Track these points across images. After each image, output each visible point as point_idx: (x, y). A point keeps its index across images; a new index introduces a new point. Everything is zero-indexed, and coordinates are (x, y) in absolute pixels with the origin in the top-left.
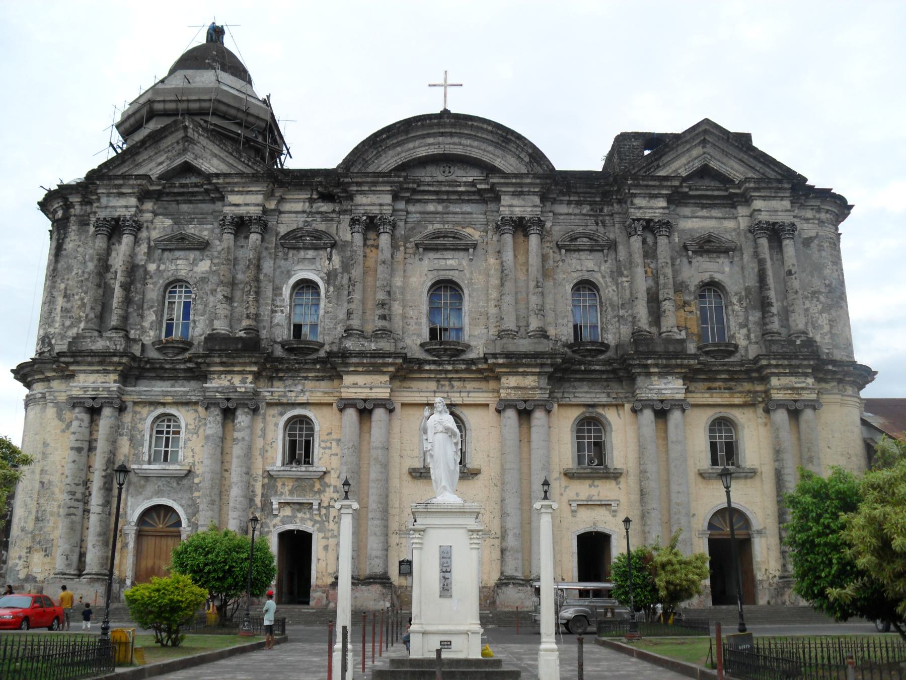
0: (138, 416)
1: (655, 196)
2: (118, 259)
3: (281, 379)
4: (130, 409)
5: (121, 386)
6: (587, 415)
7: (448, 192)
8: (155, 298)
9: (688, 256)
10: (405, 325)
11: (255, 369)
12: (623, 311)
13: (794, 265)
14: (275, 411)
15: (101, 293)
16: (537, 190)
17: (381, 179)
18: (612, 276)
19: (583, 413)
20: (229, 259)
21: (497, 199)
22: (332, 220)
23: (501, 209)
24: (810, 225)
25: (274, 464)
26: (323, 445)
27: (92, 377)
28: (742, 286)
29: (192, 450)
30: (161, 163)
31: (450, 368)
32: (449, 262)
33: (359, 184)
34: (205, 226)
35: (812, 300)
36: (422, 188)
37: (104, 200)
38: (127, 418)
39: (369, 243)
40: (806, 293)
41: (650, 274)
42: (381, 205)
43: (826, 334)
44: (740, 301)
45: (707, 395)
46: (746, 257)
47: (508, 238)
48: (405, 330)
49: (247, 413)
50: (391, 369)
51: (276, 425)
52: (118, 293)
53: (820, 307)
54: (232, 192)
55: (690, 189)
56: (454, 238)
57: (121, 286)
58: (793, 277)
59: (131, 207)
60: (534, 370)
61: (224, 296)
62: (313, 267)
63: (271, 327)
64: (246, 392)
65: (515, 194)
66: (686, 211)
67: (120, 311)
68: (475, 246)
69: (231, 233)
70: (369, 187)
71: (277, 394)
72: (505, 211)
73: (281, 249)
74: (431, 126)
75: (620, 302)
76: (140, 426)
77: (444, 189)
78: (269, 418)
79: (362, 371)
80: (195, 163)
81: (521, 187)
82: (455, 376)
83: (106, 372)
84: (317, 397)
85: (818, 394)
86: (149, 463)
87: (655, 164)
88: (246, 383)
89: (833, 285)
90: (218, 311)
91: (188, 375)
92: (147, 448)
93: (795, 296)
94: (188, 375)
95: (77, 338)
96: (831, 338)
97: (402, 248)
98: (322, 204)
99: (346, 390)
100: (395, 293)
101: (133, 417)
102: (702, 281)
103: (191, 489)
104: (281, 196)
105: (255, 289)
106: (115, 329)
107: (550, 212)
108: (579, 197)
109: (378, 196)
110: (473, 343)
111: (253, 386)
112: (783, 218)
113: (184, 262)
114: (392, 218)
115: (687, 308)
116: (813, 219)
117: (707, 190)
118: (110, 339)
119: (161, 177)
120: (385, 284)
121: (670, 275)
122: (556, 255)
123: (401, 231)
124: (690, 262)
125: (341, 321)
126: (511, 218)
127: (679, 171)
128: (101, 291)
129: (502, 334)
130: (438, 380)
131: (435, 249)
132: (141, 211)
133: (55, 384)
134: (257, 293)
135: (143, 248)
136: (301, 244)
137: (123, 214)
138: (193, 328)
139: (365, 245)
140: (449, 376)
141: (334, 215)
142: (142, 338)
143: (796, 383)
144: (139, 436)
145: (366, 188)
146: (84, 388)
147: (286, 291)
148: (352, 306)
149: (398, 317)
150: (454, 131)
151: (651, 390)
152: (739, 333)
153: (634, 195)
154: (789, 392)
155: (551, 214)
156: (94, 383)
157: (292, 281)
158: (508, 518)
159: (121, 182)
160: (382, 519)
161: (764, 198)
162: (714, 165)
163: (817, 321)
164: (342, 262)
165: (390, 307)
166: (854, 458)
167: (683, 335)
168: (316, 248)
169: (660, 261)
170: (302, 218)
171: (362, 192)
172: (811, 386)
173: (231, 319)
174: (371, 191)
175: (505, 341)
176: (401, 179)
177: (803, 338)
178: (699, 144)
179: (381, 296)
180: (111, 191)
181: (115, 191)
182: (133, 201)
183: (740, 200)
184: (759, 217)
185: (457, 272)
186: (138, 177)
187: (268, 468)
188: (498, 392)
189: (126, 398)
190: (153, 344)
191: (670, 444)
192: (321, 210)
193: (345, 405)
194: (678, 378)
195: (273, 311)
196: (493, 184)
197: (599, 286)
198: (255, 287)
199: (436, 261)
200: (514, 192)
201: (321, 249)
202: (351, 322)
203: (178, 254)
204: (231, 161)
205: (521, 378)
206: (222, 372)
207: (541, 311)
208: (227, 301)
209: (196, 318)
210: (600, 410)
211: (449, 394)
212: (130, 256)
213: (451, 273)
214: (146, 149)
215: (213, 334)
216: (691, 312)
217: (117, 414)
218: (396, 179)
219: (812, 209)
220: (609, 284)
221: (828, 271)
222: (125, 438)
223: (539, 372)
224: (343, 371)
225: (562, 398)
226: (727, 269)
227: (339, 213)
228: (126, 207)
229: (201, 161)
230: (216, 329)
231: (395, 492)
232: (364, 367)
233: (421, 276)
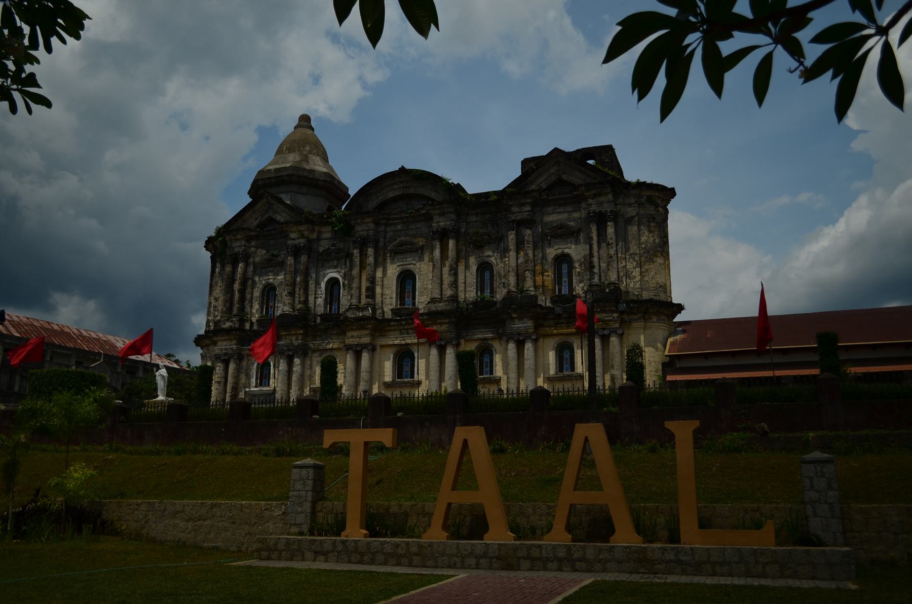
0: (250, 362)
1: (524, 204)
2: (239, 275)
3: (320, 336)
4: (245, 359)
5: (239, 347)
6: (482, 345)
8: (258, 295)
11: (302, 332)
13: (611, 239)
14: (317, 354)
16: (452, 210)
19: (480, 344)
20: (290, 271)
21: (431, 219)
23: (433, 225)
24: (632, 208)
25: (315, 384)
27: (225, 343)
30: (256, 219)
31: (404, 323)
32: (408, 259)
34: (282, 252)
35: (630, 260)
36: (391, 217)
37: (229, 244)
38: (244, 363)
42: (368, 230)
43: (638, 282)
44: (580, 265)
45: (553, 328)
48: (384, 302)
49: (298, 357)
52: (237, 295)
53: (635, 264)
56: (411, 245)
58: (610, 247)
60: (446, 321)
62: (337, 270)
63: (315, 307)
64: (298, 345)
65: (442, 214)
66: (550, 209)
67: (237, 306)
68: (422, 248)
69: (292, 256)
77: (404, 215)
82: (409, 327)
83: (231, 340)
86: (256, 387)
88: (298, 340)
90: (286, 301)
93: (610, 260)
95: (216, 323)
96: (641, 285)
97: (382, 254)
99: (348, 340)
100: (378, 282)
101: (247, 363)
102: (556, 255)
105: (303, 287)
107: (464, 222)
110: (420, 307)
111: (301, 341)
112: (607, 208)
113: (272, 274)
114: (374, 237)
115: (545, 274)
116: (634, 204)
118: (232, 321)
119: (257, 227)
122: (468, 249)
124: (550, 244)
126: (437, 230)
127: (541, 185)
128: (229, 295)
129: (433, 301)
130: (400, 330)
132: (250, 247)
133: (211, 348)
135: (251, 268)
138: (277, 311)
140: (405, 327)
142: (252, 318)
143: (606, 317)
145: (359, 222)
146: (221, 349)
147: (323, 285)
148: (353, 292)
151: (513, 328)
152: (578, 286)
153: (511, 206)
154: (601, 323)
155: (465, 224)
156: (225, 346)
157: (326, 279)
161: (595, 196)
162: (564, 177)
166: (653, 364)
172: (616, 319)
173: (293, 306)
175: (430, 305)
177: (612, 288)
182: (243, 242)
184: (591, 209)
185: (412, 265)
186: (243, 229)
187: (311, 386)
189: (244, 353)
190: (257, 321)
193: (348, 348)
194: (530, 320)
195: (316, 298)
202: (352, 301)
203: (269, 269)
205: (439, 326)
206: (286, 335)
207: (454, 284)
208: (289, 295)
209: (278, 305)
210: (490, 342)
212: (243, 274)
213: (409, 266)
215: (283, 314)
216: (548, 276)
217: (238, 362)
219: (635, 197)
220: (499, 263)
221: (645, 238)
225: (466, 336)
228: (240, 246)
230: (283, 311)
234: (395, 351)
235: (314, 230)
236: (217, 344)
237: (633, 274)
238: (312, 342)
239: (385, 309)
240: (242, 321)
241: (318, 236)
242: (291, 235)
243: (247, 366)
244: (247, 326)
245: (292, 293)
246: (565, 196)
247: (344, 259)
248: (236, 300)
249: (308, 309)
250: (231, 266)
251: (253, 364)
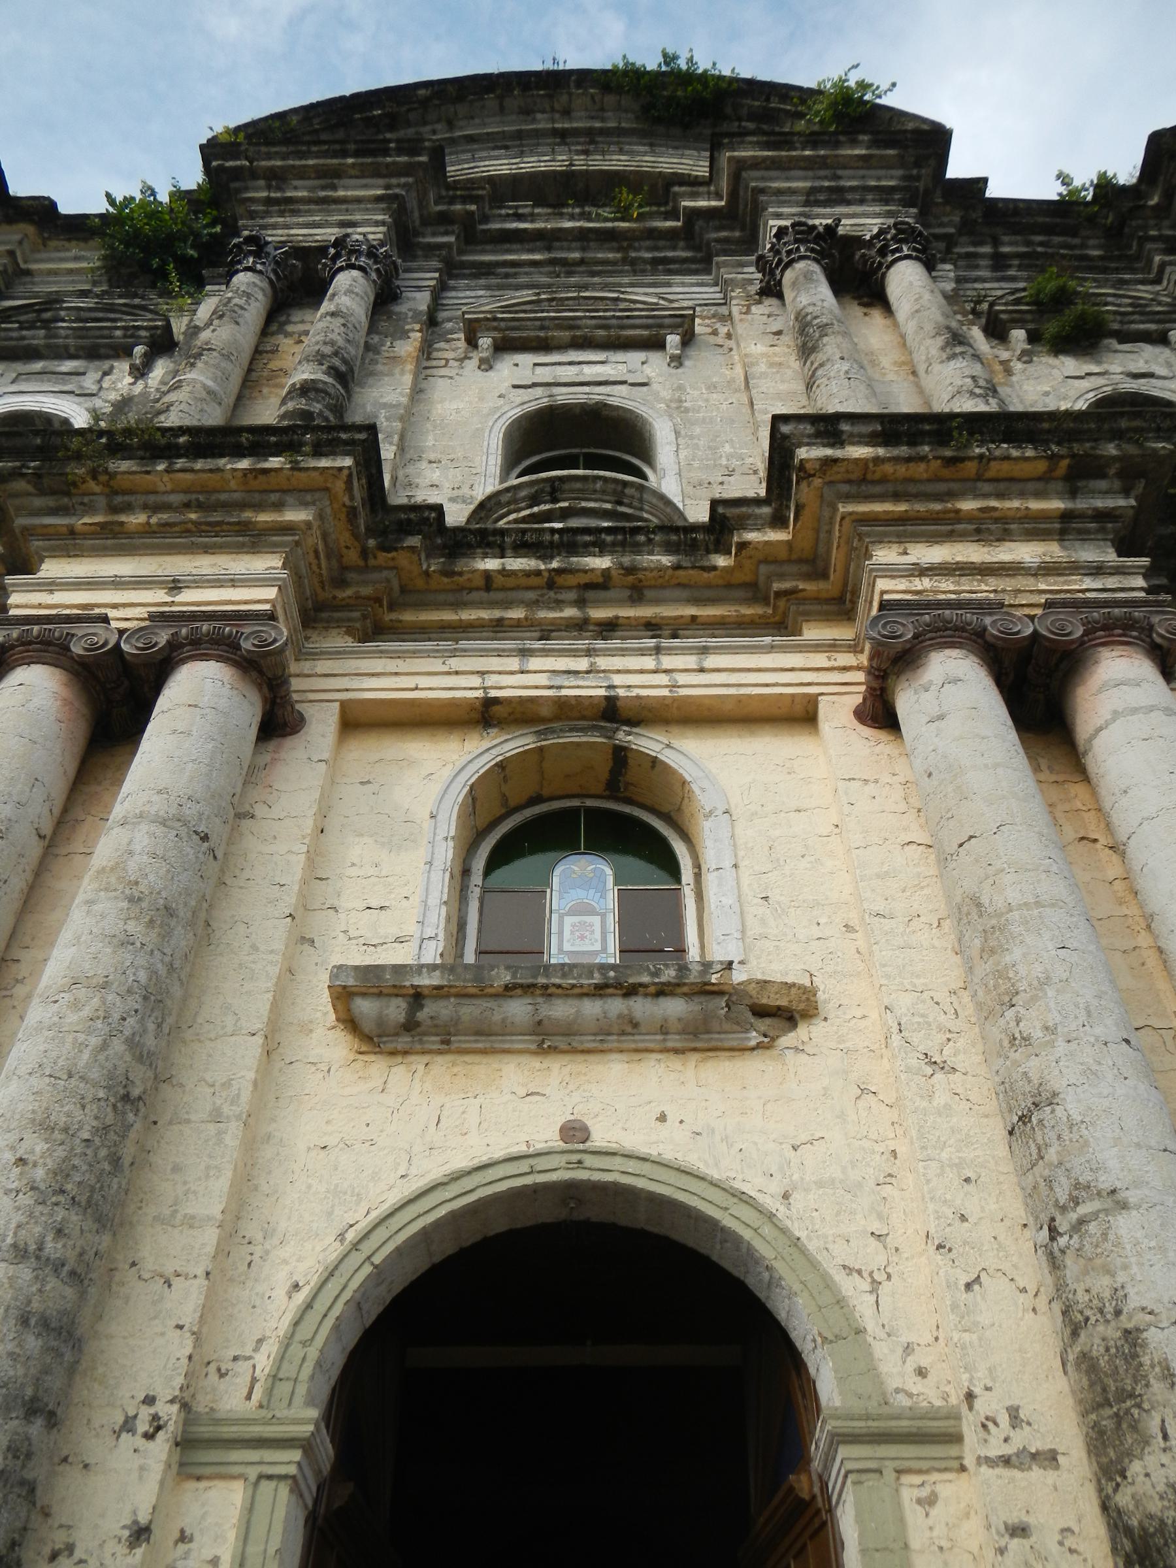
7: (583, 236)
33: (276, 178)
36: (496, 226)
50: (296, 515)
70: (311, 189)
74: (527, 112)
79: (147, 531)
108: (1028, 243)
131: (543, 346)
136: (37, 337)
140: (599, 613)
150: (598, 125)
158: (1125, 1225)
160: (20, 1253)
171: (288, 206)
199: (539, 370)
200: (812, 191)
211: (603, 662)
223: (1066, 516)
224: (48, 534)
231: (217, 1117)
232: (156, 508)
233: (481, 399)
247: (139, 350)
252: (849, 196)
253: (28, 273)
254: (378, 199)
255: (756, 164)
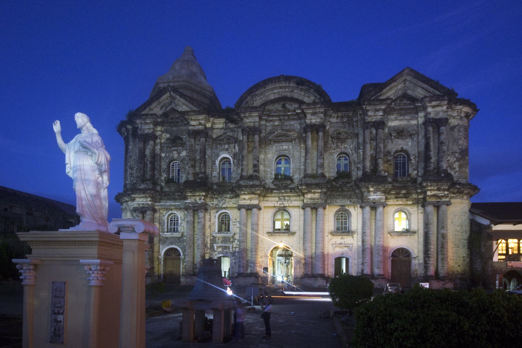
3: (216, 198)
9: (392, 139)
10: (265, 175)
12: (359, 165)
15: (143, 166)
16: (323, 111)
17: (253, 110)
18: (355, 150)
22: (235, 131)
23: (307, 121)
24: (455, 120)
25: (215, 231)
26: (233, 224)
28: (417, 151)
29: (183, 227)
33: (244, 113)
38: (157, 215)
39: (250, 140)
40: (449, 153)
41: (373, 148)
42: (254, 122)
46: (420, 137)
47: (309, 135)
51: (215, 216)
52: (149, 165)
54: (191, 119)
55: (395, 106)
57: (150, 163)
59: (151, 129)
61: (191, 165)
67: (150, 173)
69: (193, 138)
71: (214, 204)
72: (308, 121)
73: (214, 145)
75: (358, 161)
76: (163, 218)
78: (212, 214)
80: (176, 108)
81: (315, 110)
84: (231, 205)
85: (450, 199)
86: (168, 232)
87: (379, 94)
89: (463, 149)
91: (180, 198)
92: (166, 227)
94: (180, 198)
98: (230, 125)
101: (160, 215)
103: (183, 241)
104: (213, 121)
105: (203, 162)
106: (149, 180)
109: (253, 118)
115: (389, 163)
117: (404, 105)
120: (256, 157)
121: (382, 147)
123: (263, 135)
125: (239, 174)
126: (310, 125)
130: (279, 197)
134: (205, 163)
137: (148, 132)
139: (248, 141)
141: (236, 129)
144: (163, 222)
145: (247, 115)
146: (138, 204)
148: (243, 167)
149: (263, 171)
153: (368, 110)
159: (145, 117)
163: (453, 166)
164: (239, 149)
165: (259, 167)
167: (386, 174)
168: (228, 144)
169: (378, 141)
170: (223, 131)
171: (246, 117)
174: (250, 116)
176: (262, 109)
178: (403, 81)
179: (255, 162)
180: (142, 122)
181: (143, 122)
183: (420, 109)
186: (151, 115)
188: (304, 201)
189: (156, 207)
191: (377, 221)
192: (230, 127)
196: (303, 109)
197: (349, 154)
198: (203, 161)
200: (312, 112)
201: (231, 144)
204: (190, 106)
208: (192, 167)
212: (153, 150)
214: (154, 102)
218: (260, 109)
222: (157, 223)
226: (410, 144)
227: (238, 128)
228: (149, 129)
229: (178, 107)
234: (275, 211)
235: (209, 121)
236: (135, 201)
237: (454, 166)
238: (212, 202)
239: (267, 181)
240: (155, 183)
241: (212, 126)
242: (191, 122)
243: (159, 217)
244: (158, 188)
245: (194, 166)
246: (408, 107)
247: (234, 144)
248: (148, 169)
249: (207, 178)
250: (142, 143)
251: (164, 216)
252: (317, 113)
253: (215, 123)
254: (257, 116)
255: (306, 108)
